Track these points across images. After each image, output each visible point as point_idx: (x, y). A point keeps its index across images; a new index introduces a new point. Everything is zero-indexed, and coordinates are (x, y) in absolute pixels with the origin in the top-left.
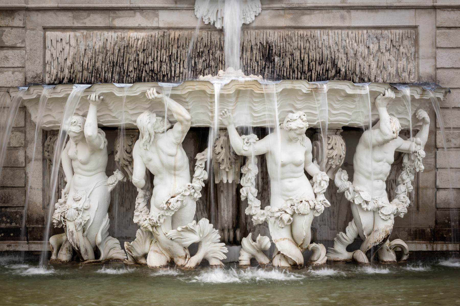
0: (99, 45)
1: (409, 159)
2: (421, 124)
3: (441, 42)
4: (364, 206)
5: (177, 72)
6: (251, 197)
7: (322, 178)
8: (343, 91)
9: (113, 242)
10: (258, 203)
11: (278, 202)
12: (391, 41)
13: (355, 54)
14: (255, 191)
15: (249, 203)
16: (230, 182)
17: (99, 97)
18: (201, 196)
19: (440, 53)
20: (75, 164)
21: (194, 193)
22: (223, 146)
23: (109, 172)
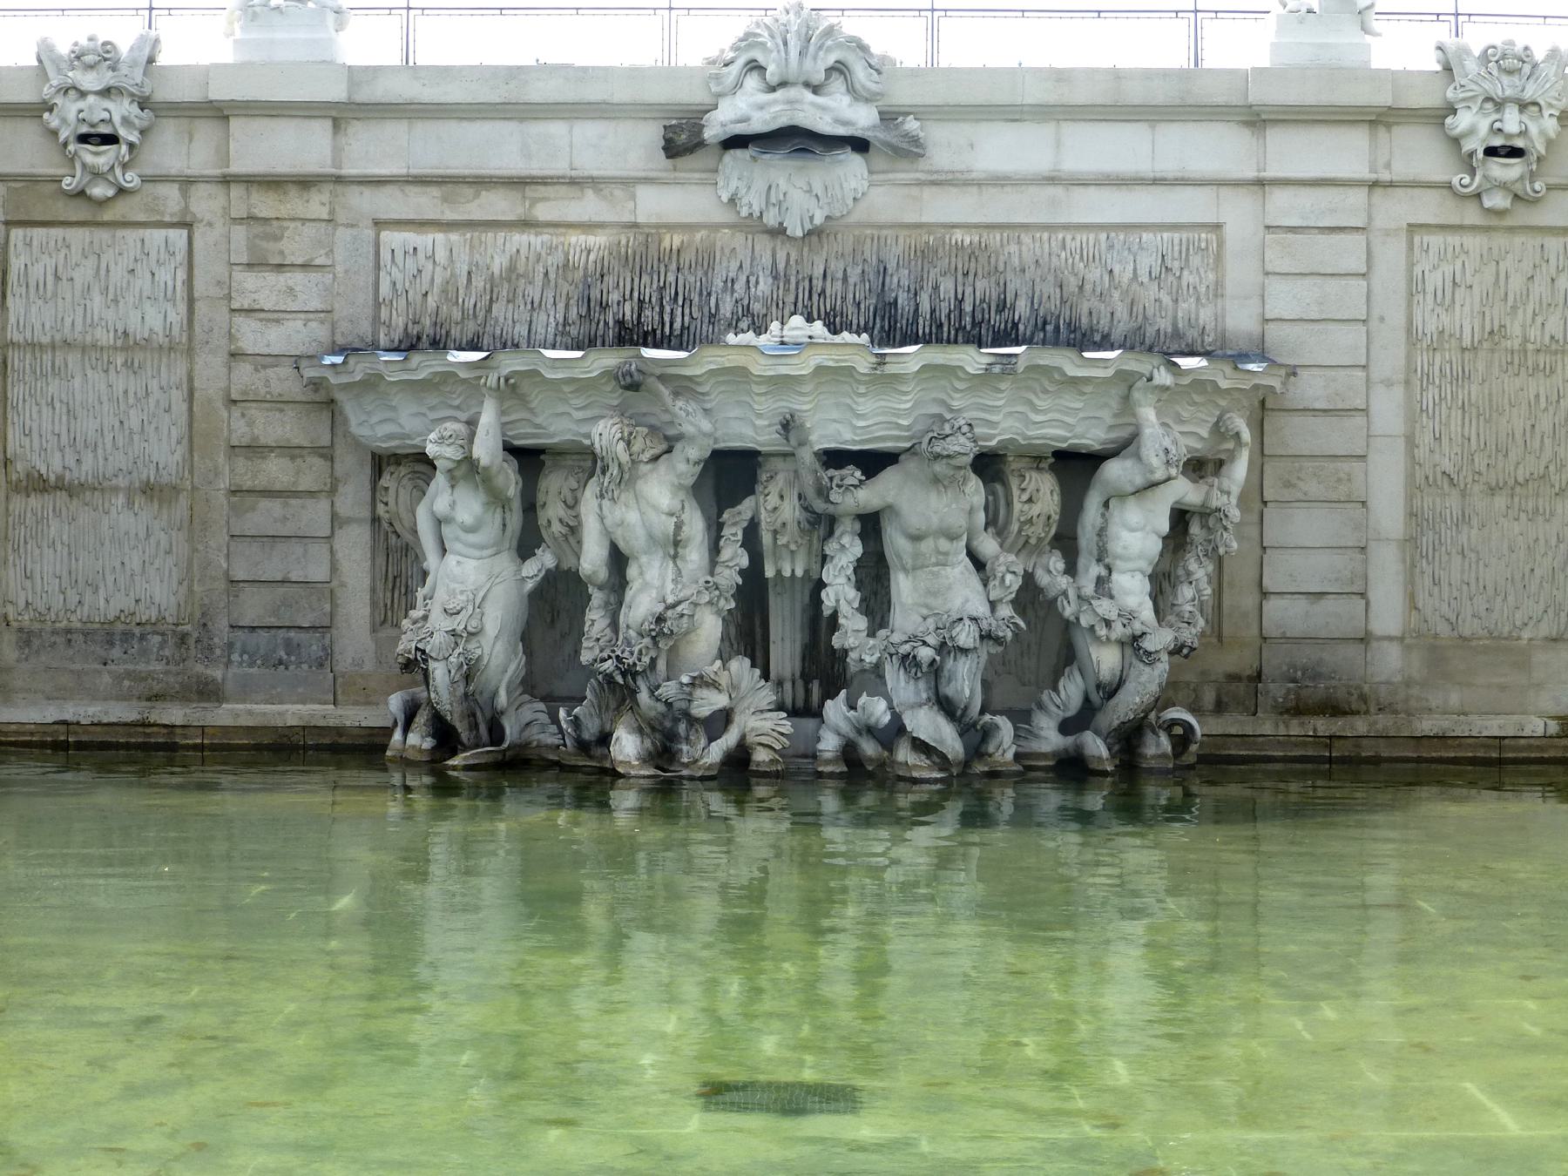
0: (498, 263)
1: (1204, 526)
2: (1230, 445)
3: (1276, 262)
4: (1102, 631)
5: (677, 325)
6: (844, 609)
7: (1009, 570)
8: (1060, 370)
9: (534, 711)
10: (861, 623)
13: (1081, 288)
14: (852, 594)
15: (841, 621)
17: (507, 380)
18: (733, 605)
19: (1276, 287)
20: (447, 531)
21: (719, 597)
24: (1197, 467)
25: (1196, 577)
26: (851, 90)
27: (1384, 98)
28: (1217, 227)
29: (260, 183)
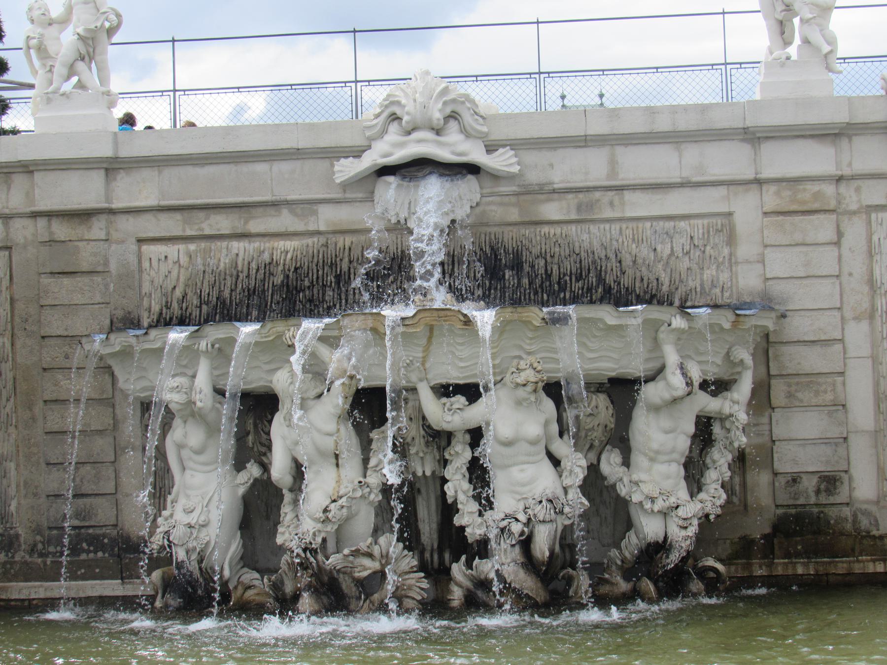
0: (225, 262)
1: (723, 427)
2: (739, 369)
3: (771, 236)
4: (648, 505)
6: (461, 497)
7: (576, 465)
8: (601, 320)
9: (250, 576)
10: (474, 507)
11: (505, 503)
12: (692, 238)
13: (634, 262)
15: (460, 506)
16: (428, 473)
17: (213, 346)
18: (380, 497)
19: (770, 253)
20: (185, 453)
21: (370, 493)
22: (412, 416)
23: (239, 466)
24: (718, 386)
25: (719, 463)
26: (466, 132)
27: (841, 117)
28: (730, 214)
29: (57, 216)
